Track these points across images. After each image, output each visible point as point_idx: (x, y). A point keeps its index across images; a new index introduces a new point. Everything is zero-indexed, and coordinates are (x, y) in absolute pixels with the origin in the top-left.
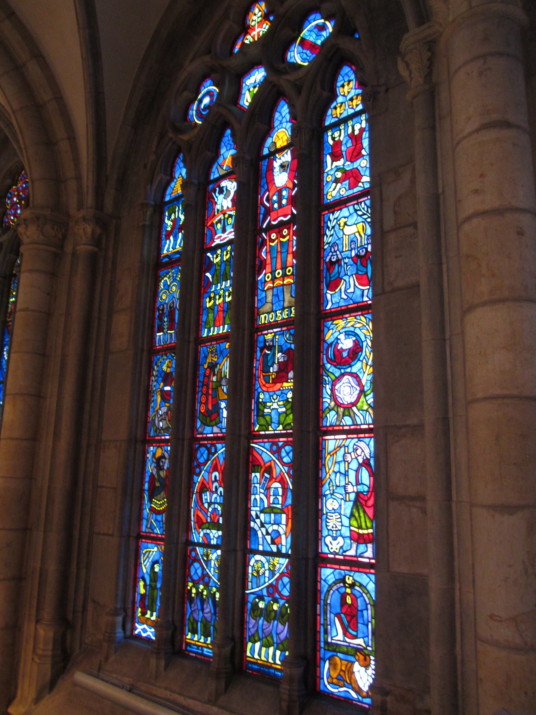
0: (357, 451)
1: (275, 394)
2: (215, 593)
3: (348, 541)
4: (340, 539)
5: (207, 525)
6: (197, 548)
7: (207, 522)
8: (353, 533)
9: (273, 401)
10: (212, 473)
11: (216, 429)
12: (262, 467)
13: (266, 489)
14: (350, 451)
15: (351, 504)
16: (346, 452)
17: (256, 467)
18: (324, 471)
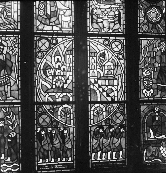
0: (161, 47)
1: (106, 10)
2: (63, 131)
3: (156, 91)
4: (152, 90)
5: (52, 90)
6: (44, 105)
7: (52, 88)
8: (158, 86)
9: (105, 15)
10: (54, 57)
11: (55, 28)
12: (97, 54)
13: (102, 66)
14: (156, 46)
15: (157, 72)
16: (154, 47)
17: (93, 54)
18: (141, 56)
